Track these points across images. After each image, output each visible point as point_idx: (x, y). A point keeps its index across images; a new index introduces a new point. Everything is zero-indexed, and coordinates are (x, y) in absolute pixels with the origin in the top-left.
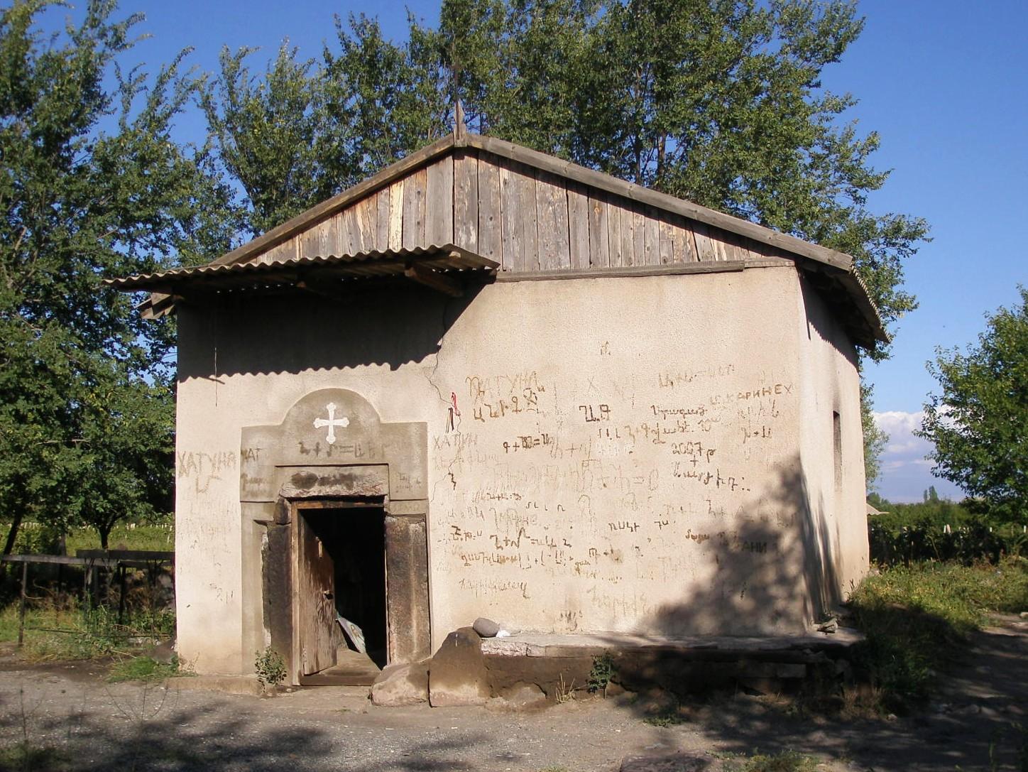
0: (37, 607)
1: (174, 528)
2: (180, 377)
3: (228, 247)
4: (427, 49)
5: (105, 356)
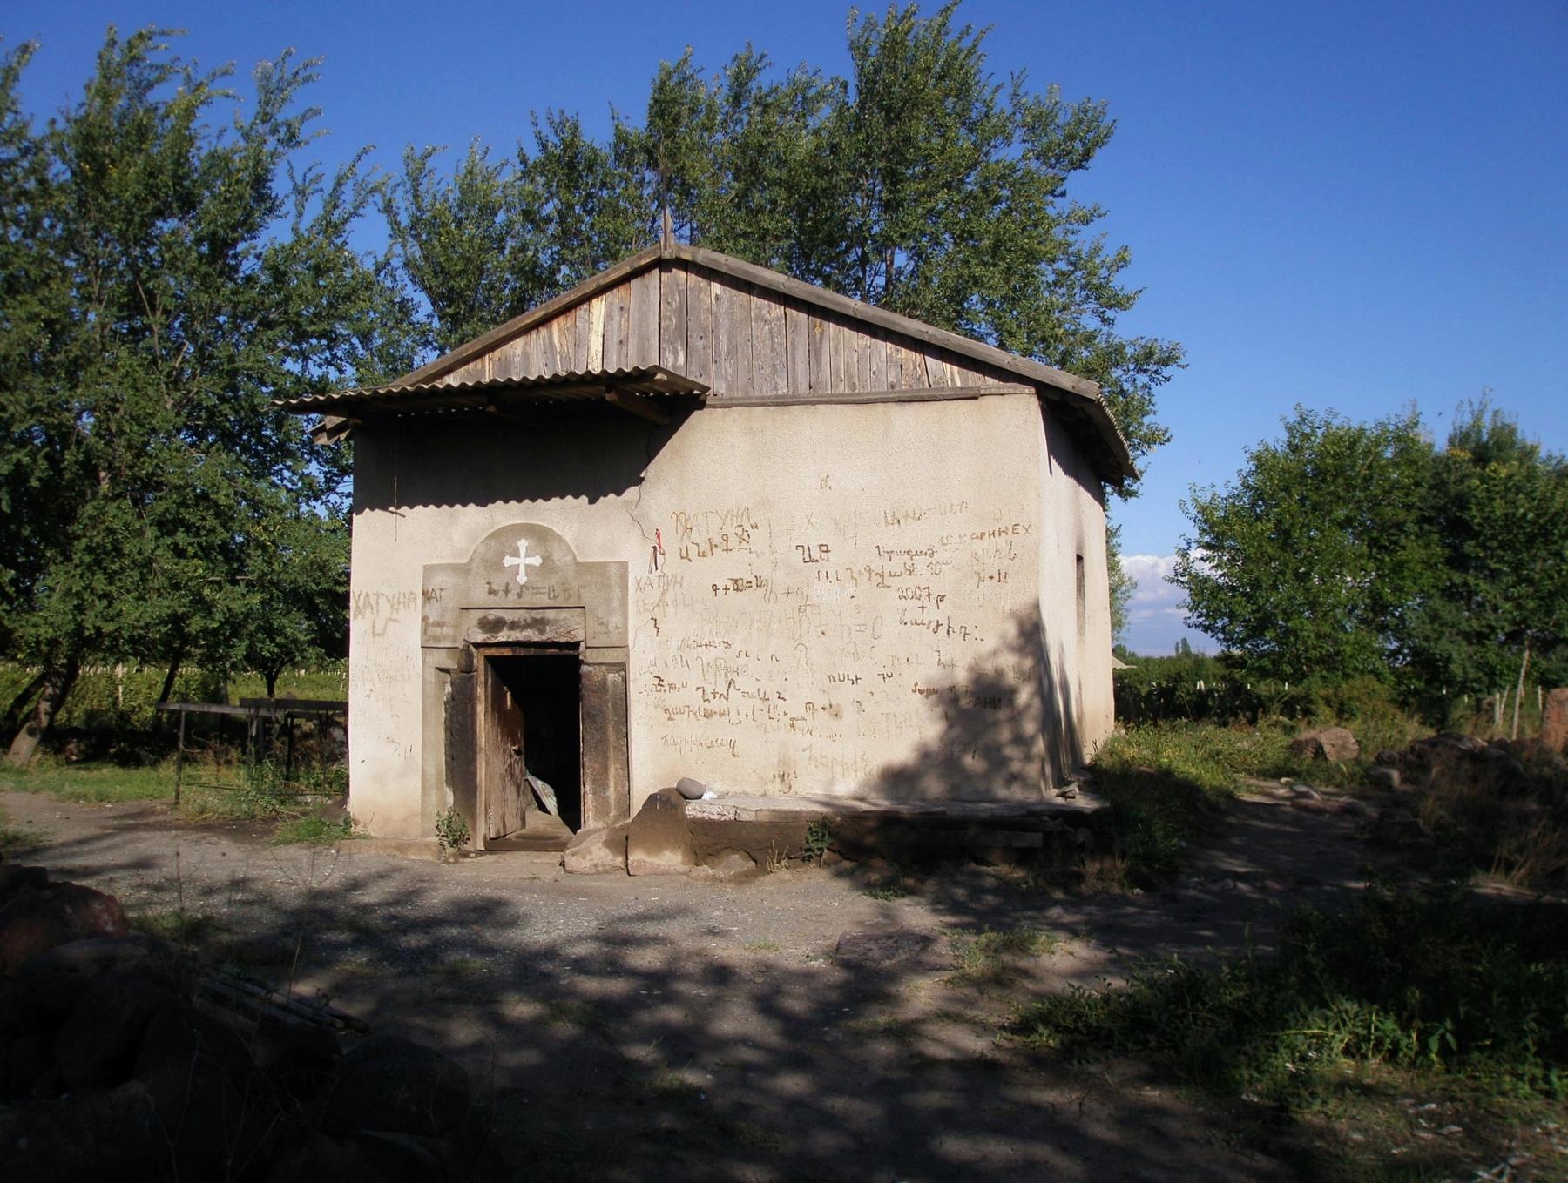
0: (196, 761)
1: (348, 676)
2: (357, 508)
3: (410, 366)
4: (633, 150)
5: (273, 484)
